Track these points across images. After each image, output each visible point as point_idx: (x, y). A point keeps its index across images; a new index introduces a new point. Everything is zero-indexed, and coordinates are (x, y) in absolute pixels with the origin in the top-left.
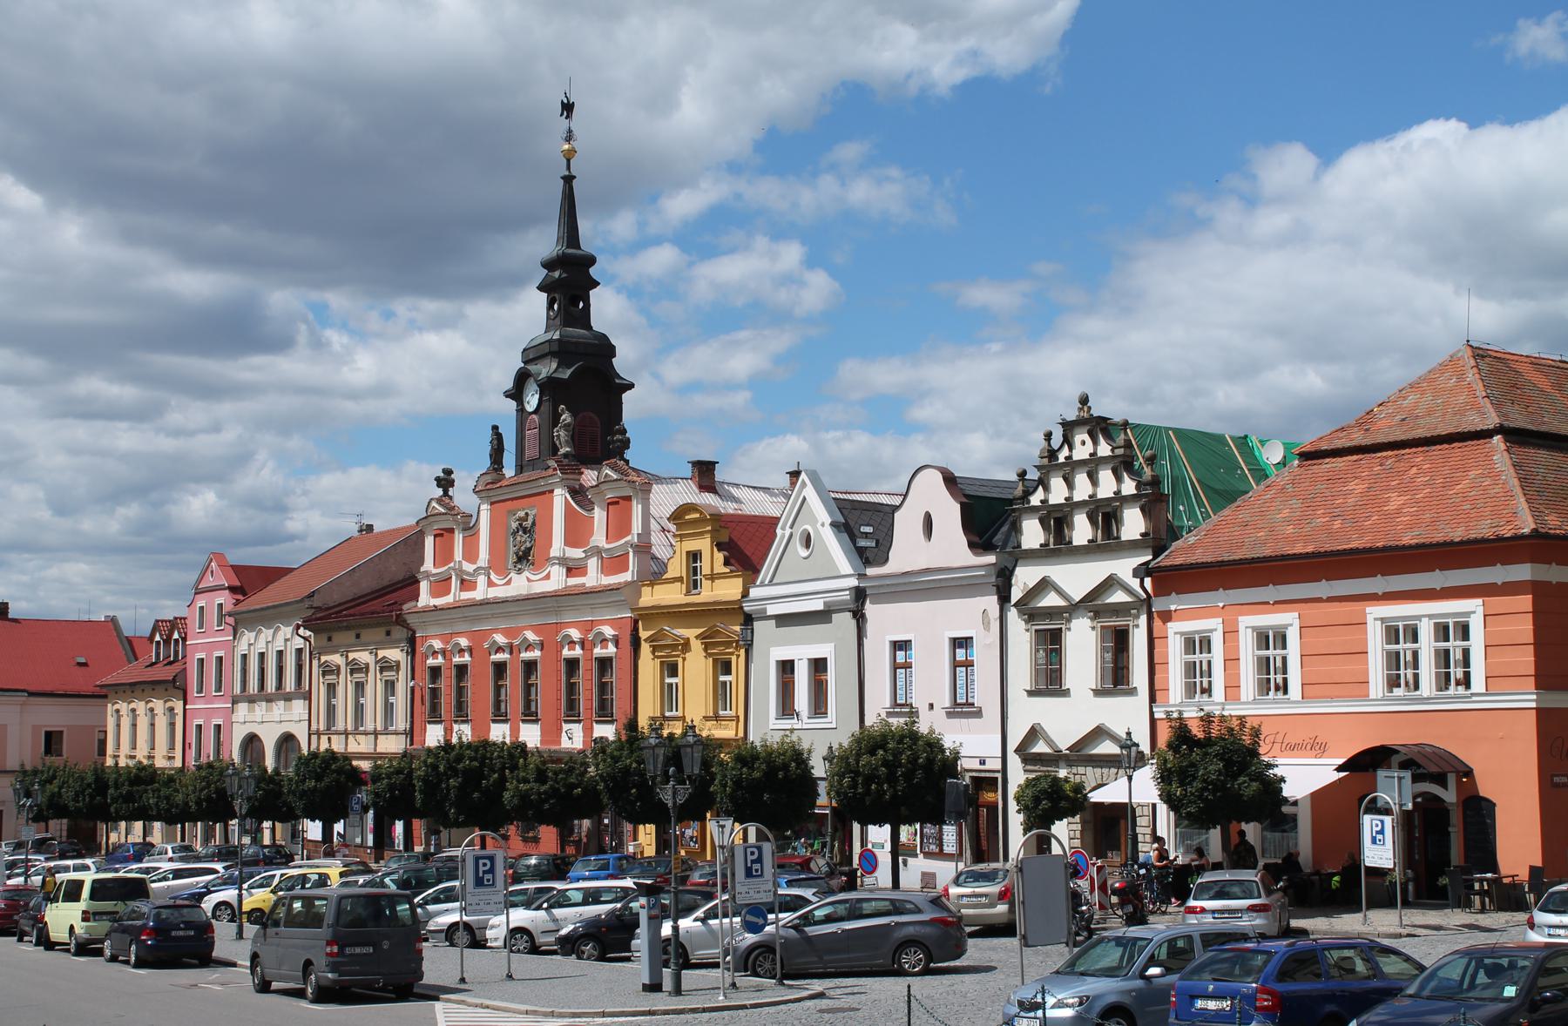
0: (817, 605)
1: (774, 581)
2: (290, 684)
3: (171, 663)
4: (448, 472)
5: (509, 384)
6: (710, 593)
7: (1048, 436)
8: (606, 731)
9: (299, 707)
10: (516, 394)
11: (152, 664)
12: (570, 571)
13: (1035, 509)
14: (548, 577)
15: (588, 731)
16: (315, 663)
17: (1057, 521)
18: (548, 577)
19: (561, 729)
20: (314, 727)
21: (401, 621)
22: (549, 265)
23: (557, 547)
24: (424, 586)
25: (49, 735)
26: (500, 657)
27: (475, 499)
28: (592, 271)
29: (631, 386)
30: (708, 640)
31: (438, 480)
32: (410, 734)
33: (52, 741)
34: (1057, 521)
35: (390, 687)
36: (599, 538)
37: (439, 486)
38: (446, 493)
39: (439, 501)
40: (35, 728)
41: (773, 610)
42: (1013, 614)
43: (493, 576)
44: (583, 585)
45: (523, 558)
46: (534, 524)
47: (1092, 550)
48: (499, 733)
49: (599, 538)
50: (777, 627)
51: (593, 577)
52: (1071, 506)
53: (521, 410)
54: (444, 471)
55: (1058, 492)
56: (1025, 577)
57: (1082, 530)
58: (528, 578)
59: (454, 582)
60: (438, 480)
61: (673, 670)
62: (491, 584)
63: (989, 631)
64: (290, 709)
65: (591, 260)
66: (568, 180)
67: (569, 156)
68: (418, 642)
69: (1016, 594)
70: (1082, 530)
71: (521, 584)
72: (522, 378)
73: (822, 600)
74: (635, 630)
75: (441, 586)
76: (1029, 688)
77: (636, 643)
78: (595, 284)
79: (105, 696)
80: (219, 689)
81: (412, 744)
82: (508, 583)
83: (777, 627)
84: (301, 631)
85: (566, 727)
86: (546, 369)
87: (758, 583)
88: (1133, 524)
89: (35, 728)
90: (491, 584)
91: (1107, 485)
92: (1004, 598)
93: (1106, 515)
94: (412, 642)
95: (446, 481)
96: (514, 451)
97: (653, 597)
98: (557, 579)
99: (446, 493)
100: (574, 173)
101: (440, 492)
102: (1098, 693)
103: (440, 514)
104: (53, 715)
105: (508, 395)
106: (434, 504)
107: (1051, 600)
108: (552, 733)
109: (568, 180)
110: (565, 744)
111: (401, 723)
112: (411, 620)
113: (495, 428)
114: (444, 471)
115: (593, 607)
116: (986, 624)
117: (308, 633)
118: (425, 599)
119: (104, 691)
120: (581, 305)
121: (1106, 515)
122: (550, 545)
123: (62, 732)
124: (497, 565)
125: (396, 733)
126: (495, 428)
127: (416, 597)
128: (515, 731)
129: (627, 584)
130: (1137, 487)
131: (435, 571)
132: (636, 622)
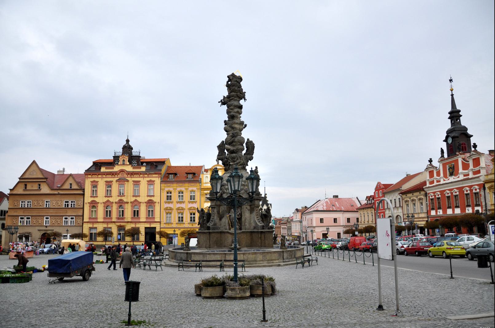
2: (398, 205)
3: (370, 204)
4: (431, 159)
5: (444, 139)
8: (479, 208)
9: (400, 210)
10: (446, 141)
11: (367, 205)
12: (465, 176)
14: (459, 177)
15: (473, 209)
16: (403, 201)
18: (459, 177)
19: (466, 209)
20: (404, 213)
21: (423, 190)
22: (449, 113)
23: (461, 170)
24: (428, 183)
25: (347, 219)
26: (448, 195)
27: (439, 164)
28: (460, 113)
29: (472, 136)
31: (429, 161)
32: (427, 213)
33: (348, 220)
35: (422, 203)
36: (471, 167)
37: (429, 162)
38: (431, 163)
39: (430, 165)
40: (345, 217)
43: (444, 179)
44: (469, 178)
45: (451, 174)
46: (454, 166)
48: (449, 212)
49: (471, 167)
51: (471, 176)
53: (447, 144)
54: (430, 159)
58: (454, 178)
59: (435, 181)
60: (429, 161)
62: (444, 180)
64: (398, 210)
65: (459, 111)
66: (452, 95)
67: (452, 90)
68: (428, 195)
71: (452, 179)
72: (447, 137)
75: (432, 182)
77: (484, 189)
78: (461, 116)
79: (358, 211)
80: (382, 208)
81: (428, 215)
82: (449, 179)
84: (400, 195)
85: (467, 208)
86: (453, 135)
89: (345, 217)
90: (444, 180)
94: (426, 195)
95: (431, 161)
96: (446, 153)
98: (461, 177)
99: (431, 163)
100: (453, 94)
101: (429, 163)
104: (348, 215)
105: (444, 141)
106: (428, 166)
108: (463, 210)
109: (452, 95)
110: (467, 212)
111: (425, 211)
112: (425, 190)
113: (441, 148)
114: (430, 159)
117: (401, 195)
118: (428, 185)
119: (358, 210)
120: (458, 120)
122: (459, 170)
123: (350, 218)
124: (445, 176)
125: (424, 213)
126: (441, 148)
127: (426, 185)
128: (453, 211)
129: (480, 176)
131: (430, 179)
132: (484, 184)
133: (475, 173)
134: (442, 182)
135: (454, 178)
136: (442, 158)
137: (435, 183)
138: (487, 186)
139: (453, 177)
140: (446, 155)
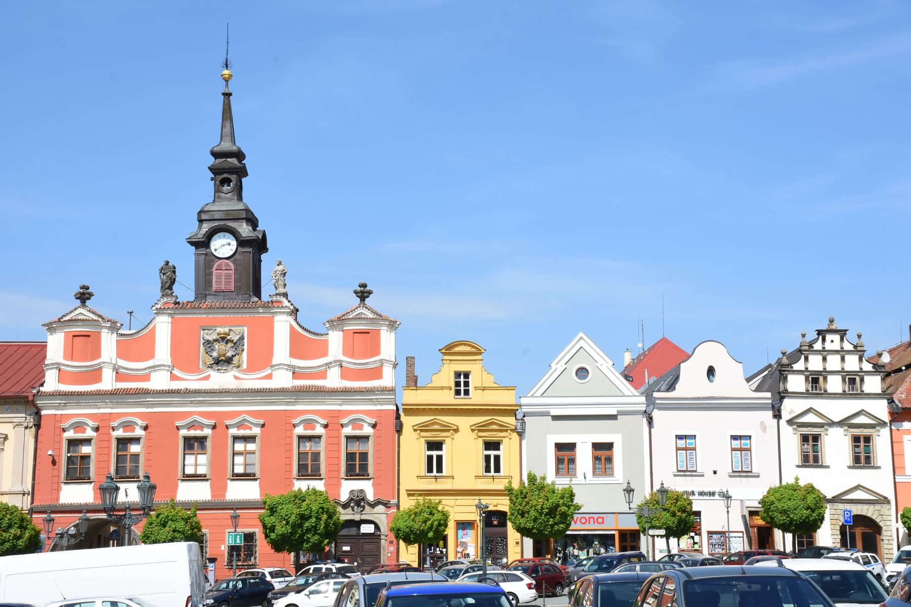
0: (612, 411)
1: (544, 395)
6: (476, 398)
7: (803, 336)
13: (799, 372)
17: (815, 380)
18: (269, 377)
21: (33, 403)
30: (479, 429)
34: (815, 380)
41: (555, 412)
42: (783, 422)
43: (176, 372)
47: (843, 395)
50: (617, 420)
51: (333, 380)
52: (825, 373)
55: (815, 363)
56: (790, 407)
57: (835, 384)
58: (236, 378)
61: (435, 445)
62: (174, 378)
63: (765, 432)
69: (786, 415)
70: (835, 384)
73: (616, 409)
74: (398, 417)
76: (798, 464)
77: (399, 429)
83: (617, 420)
87: (530, 395)
88: (873, 384)
90: (174, 378)
91: (852, 364)
92: (778, 416)
93: (852, 380)
97: (411, 397)
98: (282, 380)
101: (78, 302)
102: (850, 467)
103: (93, 320)
107: (810, 418)
115: (345, 402)
116: (763, 428)
121: (852, 380)
130: (873, 367)
133: (346, 374)
134: (160, 381)
135: (236, 378)
136: (171, 300)
137: (108, 382)
138: (408, 422)
139: (235, 372)
140: (185, 290)
